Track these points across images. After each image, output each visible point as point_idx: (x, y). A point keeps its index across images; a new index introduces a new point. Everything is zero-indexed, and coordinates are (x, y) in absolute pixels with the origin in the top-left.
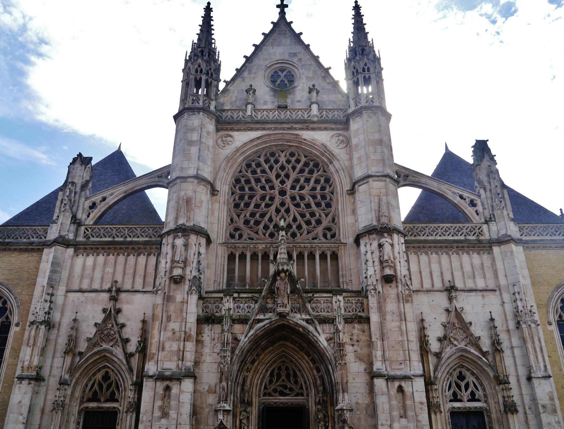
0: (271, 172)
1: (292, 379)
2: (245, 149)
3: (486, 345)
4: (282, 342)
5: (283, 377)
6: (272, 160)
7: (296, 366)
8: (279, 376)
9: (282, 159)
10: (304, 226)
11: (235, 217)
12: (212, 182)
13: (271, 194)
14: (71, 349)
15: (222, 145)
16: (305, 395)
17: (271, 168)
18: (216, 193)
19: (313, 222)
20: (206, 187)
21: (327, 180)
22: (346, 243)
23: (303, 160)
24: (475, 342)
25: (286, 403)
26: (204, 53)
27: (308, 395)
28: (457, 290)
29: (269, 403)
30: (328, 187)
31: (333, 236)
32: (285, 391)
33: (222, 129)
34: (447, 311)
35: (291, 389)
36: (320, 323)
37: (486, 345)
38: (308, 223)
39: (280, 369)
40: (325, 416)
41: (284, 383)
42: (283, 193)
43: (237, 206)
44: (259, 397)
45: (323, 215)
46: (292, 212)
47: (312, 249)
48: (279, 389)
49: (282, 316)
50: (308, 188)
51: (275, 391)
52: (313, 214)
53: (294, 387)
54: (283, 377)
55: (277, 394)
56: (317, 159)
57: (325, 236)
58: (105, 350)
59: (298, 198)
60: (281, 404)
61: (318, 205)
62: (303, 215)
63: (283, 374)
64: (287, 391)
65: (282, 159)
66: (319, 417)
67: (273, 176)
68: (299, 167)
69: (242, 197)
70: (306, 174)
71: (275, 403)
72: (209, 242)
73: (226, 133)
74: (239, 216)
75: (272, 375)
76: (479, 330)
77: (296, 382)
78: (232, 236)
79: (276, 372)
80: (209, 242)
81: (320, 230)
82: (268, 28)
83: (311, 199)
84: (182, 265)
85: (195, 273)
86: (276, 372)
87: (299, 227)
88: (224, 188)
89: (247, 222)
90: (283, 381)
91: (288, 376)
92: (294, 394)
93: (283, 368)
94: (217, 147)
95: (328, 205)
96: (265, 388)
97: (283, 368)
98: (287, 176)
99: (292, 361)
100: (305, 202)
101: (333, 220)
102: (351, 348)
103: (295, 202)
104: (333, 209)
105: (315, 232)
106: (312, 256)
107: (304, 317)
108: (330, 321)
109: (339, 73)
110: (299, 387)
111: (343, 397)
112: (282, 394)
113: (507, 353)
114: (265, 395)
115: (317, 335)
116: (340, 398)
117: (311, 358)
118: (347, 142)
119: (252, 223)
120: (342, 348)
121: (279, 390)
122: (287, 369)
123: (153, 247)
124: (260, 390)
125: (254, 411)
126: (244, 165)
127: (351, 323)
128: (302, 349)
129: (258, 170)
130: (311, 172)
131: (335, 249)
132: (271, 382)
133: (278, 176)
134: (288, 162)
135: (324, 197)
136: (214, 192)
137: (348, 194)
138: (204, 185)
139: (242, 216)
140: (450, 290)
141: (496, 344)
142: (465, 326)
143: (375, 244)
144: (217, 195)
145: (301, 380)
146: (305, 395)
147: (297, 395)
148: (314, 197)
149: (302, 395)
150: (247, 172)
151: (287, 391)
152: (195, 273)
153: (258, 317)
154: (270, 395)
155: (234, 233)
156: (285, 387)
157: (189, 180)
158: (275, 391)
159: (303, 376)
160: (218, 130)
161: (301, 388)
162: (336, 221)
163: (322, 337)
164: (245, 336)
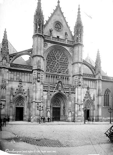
3: (92, 99)
14: (12, 94)
24: (91, 98)
26: (39, 15)
28: (89, 88)
31: (68, 73)
34: (87, 92)
37: (92, 99)
49: (60, 91)
58: (20, 95)
68: (62, 55)
76: (92, 96)
78: (47, 71)
82: (55, 8)
88: (45, 58)
109: (72, 29)
113: (95, 100)
118: (73, 52)
123: (32, 72)
133: (57, 56)
140: (88, 88)
141: (94, 99)
142: (89, 95)
143: (78, 78)
155: (47, 70)
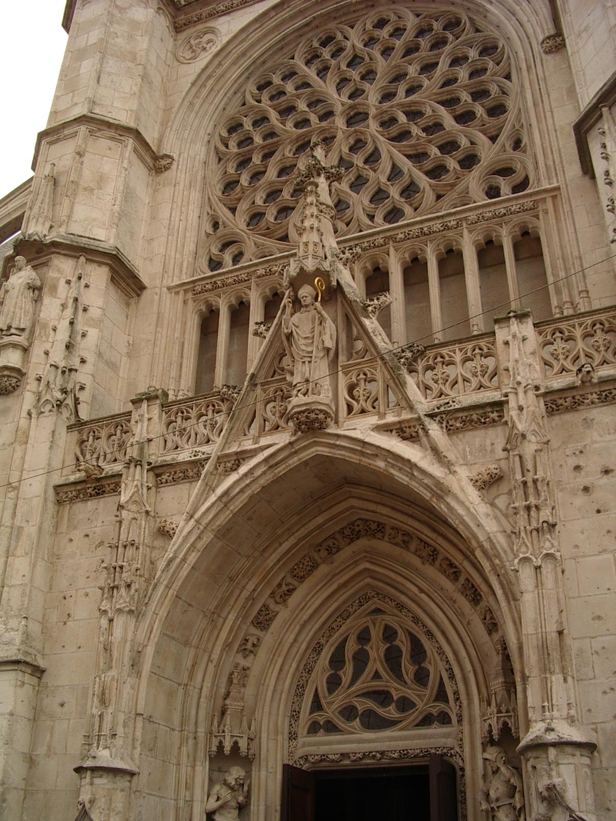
0: (325, 82)
1: (408, 669)
2: (246, 45)
4: (363, 543)
5: (376, 662)
6: (326, 53)
7: (416, 620)
8: (361, 660)
9: (355, 40)
10: (424, 181)
11: (224, 213)
12: (132, 124)
13: (323, 130)
15: (188, 55)
16: (454, 719)
17: (323, 72)
18: (163, 162)
19: (452, 164)
20: (120, 141)
21: (489, 49)
22: (557, 189)
23: (411, 22)
25: (383, 753)
27: (460, 721)
29: (324, 758)
30: (491, 65)
32: (380, 711)
33: (188, 24)
35: (405, 705)
36: (450, 431)
38: (437, 172)
39: (364, 637)
40: (512, 791)
41: (377, 685)
42: (356, 117)
43: (230, 185)
44: (293, 736)
45: (482, 139)
46: (384, 156)
47: (450, 234)
48: (363, 705)
49: (311, 424)
50: (431, 84)
51: (349, 712)
52: (449, 147)
53: (411, 694)
54: (376, 662)
55: (357, 723)
56: (452, 8)
57: (493, 192)
59: (402, 118)
60: (365, 756)
61: (465, 118)
62: (418, 157)
63: (376, 650)
64: (391, 712)
65: (355, 40)
66: (493, 795)
67: (328, 88)
69: (244, 163)
70: (424, 53)
71: (344, 755)
72: (126, 280)
73: (200, 27)
74: (233, 210)
75: (337, 661)
77: (421, 677)
78: (215, 264)
79: (351, 647)
80: (126, 280)
81: (474, 181)
83: (442, 111)
84: (21, 339)
85: (58, 356)
86: (351, 647)
87: (410, 190)
88: (192, 150)
89: (256, 217)
90: (377, 676)
91: (392, 659)
92: (414, 716)
93: (376, 633)
94: (176, 63)
95: (497, 110)
96: (317, 705)
97: (376, 633)
98: (369, 75)
99: (401, 606)
100: (423, 122)
101: (517, 144)
102: (580, 500)
103: (394, 131)
104: (511, 116)
105: (459, 188)
106: (451, 260)
107: (390, 418)
108: (491, 413)
110: (430, 691)
111: (547, 694)
112: (373, 722)
114: (314, 728)
115: (437, 471)
116: (533, 696)
117: (462, 580)
119: (270, 216)
120: (532, 500)
121: (360, 709)
122: (389, 634)
124: (295, 715)
125: (268, 785)
126: (251, 87)
127: (575, 406)
128: (406, 539)
129: (290, 87)
130: (438, 44)
131: (526, 217)
132: (333, 683)
134: (370, 42)
135: (479, 94)
136: (158, 163)
137: (546, 53)
138: (112, 139)
139: (243, 206)
144: (167, 168)
145: (435, 667)
146: (454, 719)
147: (426, 721)
148: (450, 103)
149: (444, 719)
150: (259, 101)
151: (391, 712)
152: (58, 356)
153: (234, 449)
154: (331, 728)
156: (383, 697)
157: (67, 132)
158: (349, 712)
159: (441, 652)
160: (178, 29)
161: (441, 695)
162: (525, 140)
163: (455, 475)
164: (187, 510)
